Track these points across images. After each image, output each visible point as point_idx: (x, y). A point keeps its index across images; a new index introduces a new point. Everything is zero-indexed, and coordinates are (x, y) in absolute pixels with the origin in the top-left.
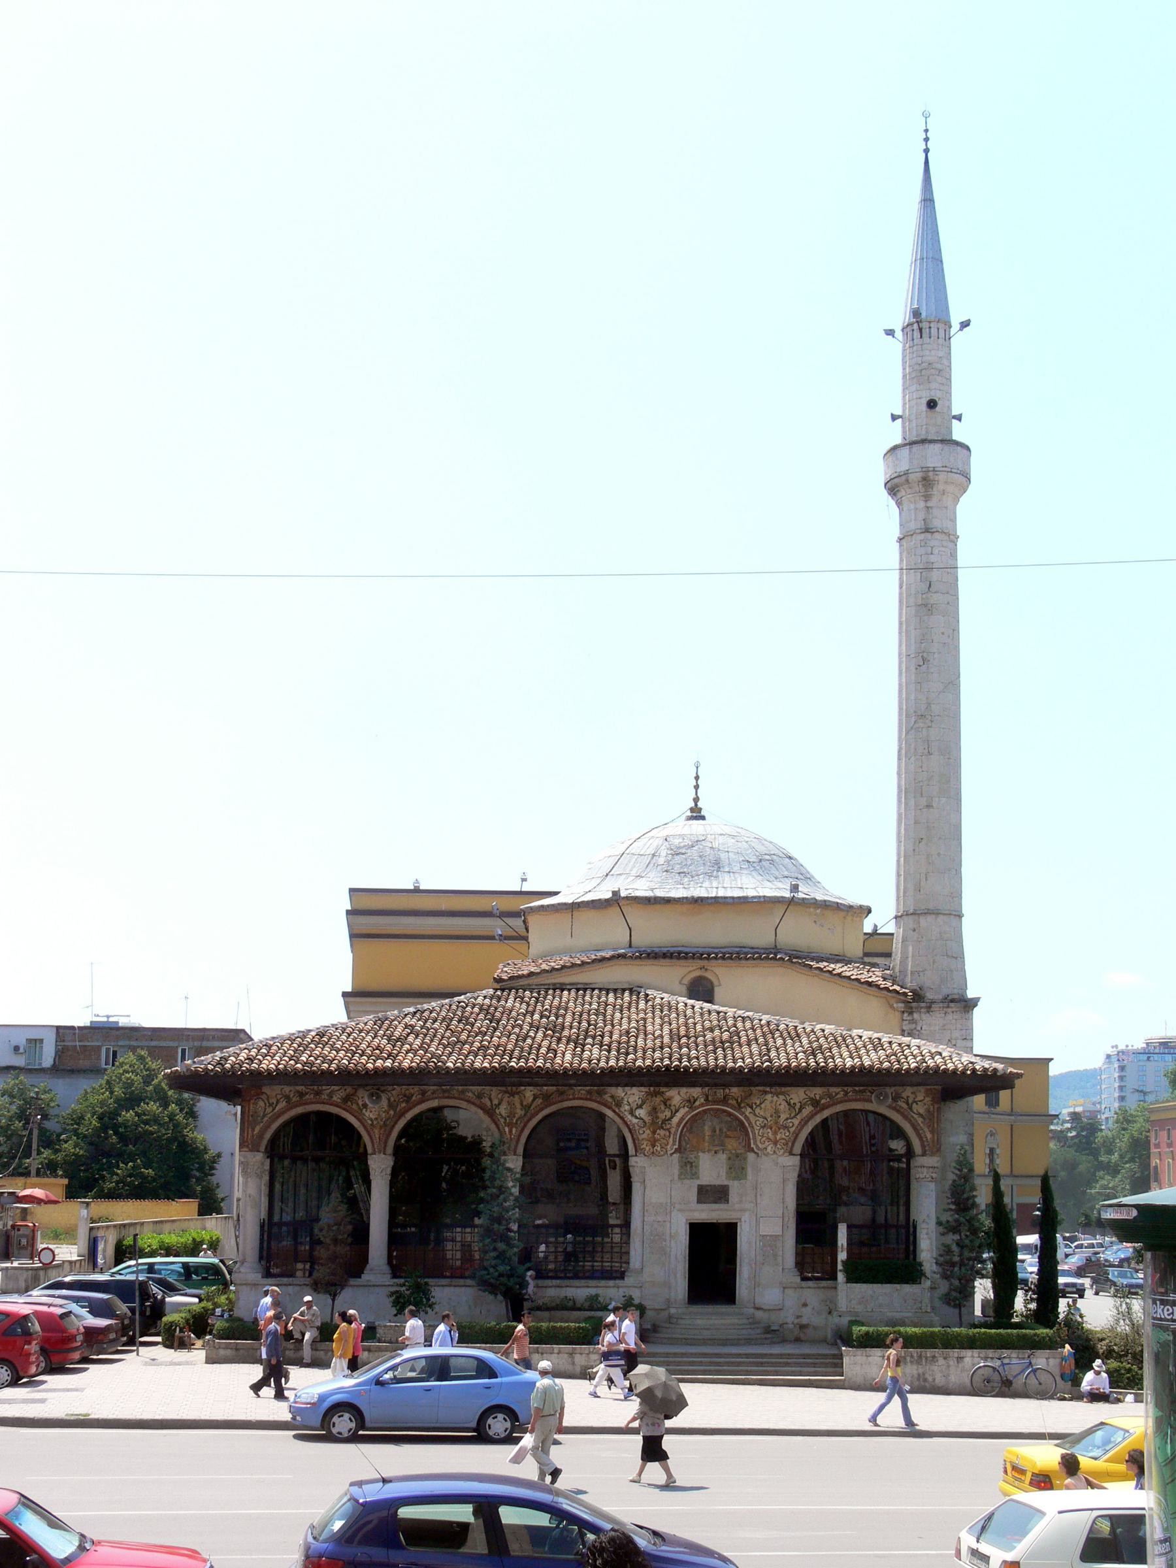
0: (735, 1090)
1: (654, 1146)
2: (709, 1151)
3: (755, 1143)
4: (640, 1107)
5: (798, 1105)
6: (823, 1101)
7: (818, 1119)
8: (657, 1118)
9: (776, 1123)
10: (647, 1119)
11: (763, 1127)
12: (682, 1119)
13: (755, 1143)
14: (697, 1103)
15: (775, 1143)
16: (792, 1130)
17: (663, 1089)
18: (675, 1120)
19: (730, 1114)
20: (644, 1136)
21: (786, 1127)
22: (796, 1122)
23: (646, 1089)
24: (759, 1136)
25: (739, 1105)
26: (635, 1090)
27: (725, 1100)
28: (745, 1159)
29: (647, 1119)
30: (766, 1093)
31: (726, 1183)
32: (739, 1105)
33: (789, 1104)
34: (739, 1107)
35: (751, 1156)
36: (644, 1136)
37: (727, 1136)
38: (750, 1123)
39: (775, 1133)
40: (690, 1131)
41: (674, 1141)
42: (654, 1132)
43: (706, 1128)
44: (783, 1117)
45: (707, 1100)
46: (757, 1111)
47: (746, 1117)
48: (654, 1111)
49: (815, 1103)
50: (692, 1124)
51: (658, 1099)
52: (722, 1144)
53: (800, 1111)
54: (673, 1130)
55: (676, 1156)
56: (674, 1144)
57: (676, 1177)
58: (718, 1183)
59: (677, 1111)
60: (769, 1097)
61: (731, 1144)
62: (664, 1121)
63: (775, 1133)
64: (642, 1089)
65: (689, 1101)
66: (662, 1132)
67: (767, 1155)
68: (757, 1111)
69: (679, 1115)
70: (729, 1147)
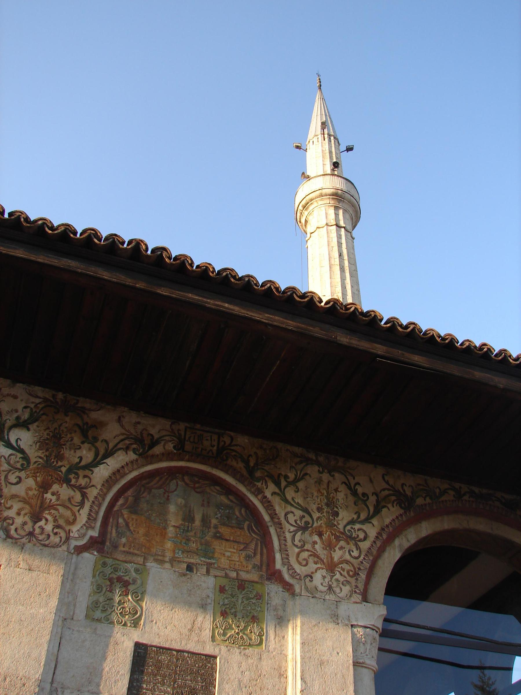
0: (242, 440)
1: (36, 518)
2: (173, 561)
3: (286, 561)
4: (24, 425)
5: (372, 499)
6: (419, 501)
7: (410, 538)
8: (60, 457)
9: (331, 525)
10: (33, 454)
11: (304, 529)
12: (118, 473)
13: (286, 561)
14: (158, 450)
15: (331, 567)
16: (365, 545)
17: (85, 403)
18: (102, 472)
19: (228, 490)
20: (20, 490)
21: (356, 540)
22: (372, 532)
23: (47, 394)
24: (295, 548)
25: (251, 472)
26: (19, 389)
27: (220, 458)
28: (259, 597)
29: (33, 454)
30: (308, 461)
31: (209, 649)
32: (251, 472)
33: (354, 493)
34: (249, 477)
35: (274, 592)
36: (20, 490)
37: (219, 537)
38: (273, 515)
39: (330, 546)
40: (134, 509)
41: (91, 519)
42: (45, 487)
43: (172, 508)
44: (344, 516)
45: (180, 446)
46: (290, 493)
47: (268, 505)
48: (53, 444)
49: (405, 502)
50: (136, 494)
51: (69, 421)
52: (207, 552)
53: (377, 511)
54: (93, 493)
55: (89, 558)
56: (89, 526)
57: (80, 612)
58: (192, 646)
59: (109, 454)
60: (313, 470)
61: (228, 555)
62: (74, 469)
63: (330, 546)
64: (38, 390)
65: (139, 440)
66: (65, 491)
67: (313, 593)
68: (290, 493)
69: (113, 463)
70: (224, 562)
